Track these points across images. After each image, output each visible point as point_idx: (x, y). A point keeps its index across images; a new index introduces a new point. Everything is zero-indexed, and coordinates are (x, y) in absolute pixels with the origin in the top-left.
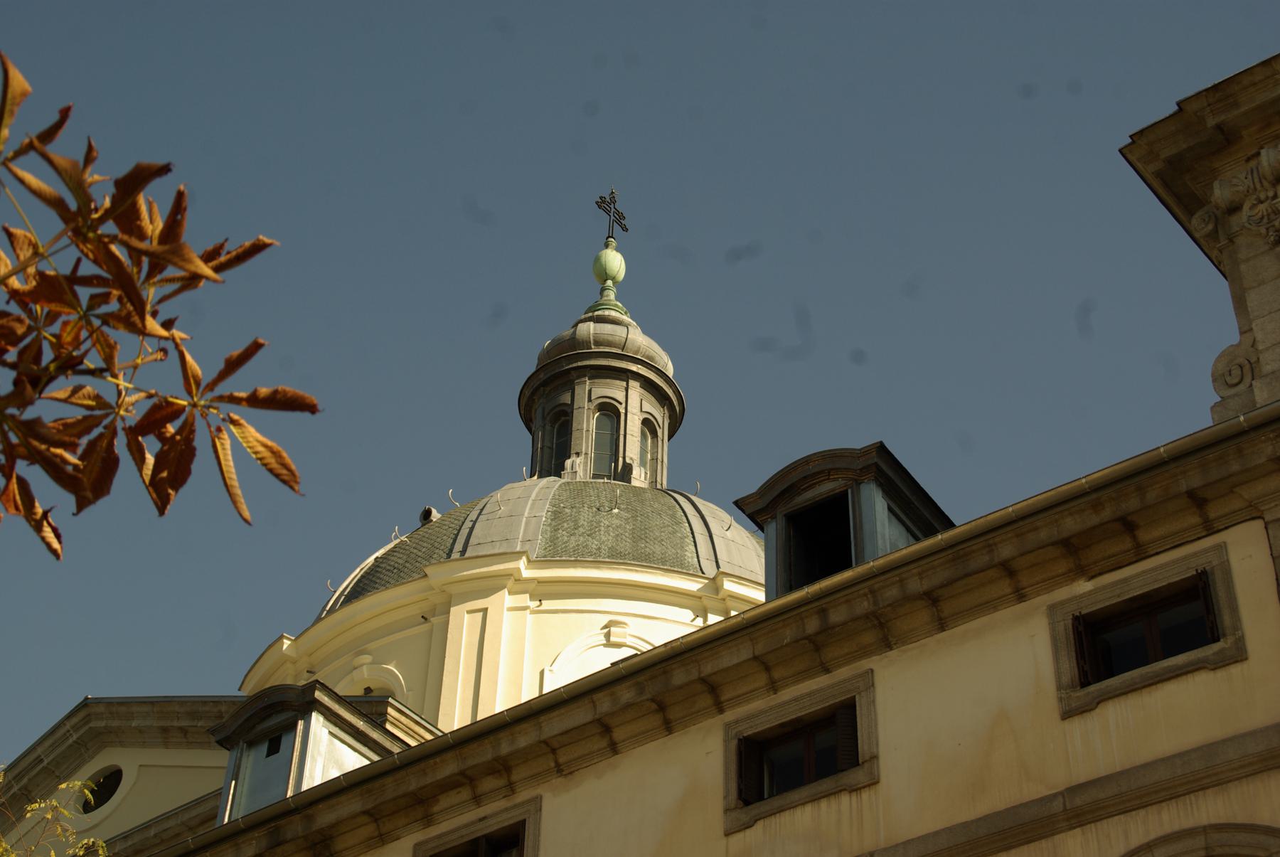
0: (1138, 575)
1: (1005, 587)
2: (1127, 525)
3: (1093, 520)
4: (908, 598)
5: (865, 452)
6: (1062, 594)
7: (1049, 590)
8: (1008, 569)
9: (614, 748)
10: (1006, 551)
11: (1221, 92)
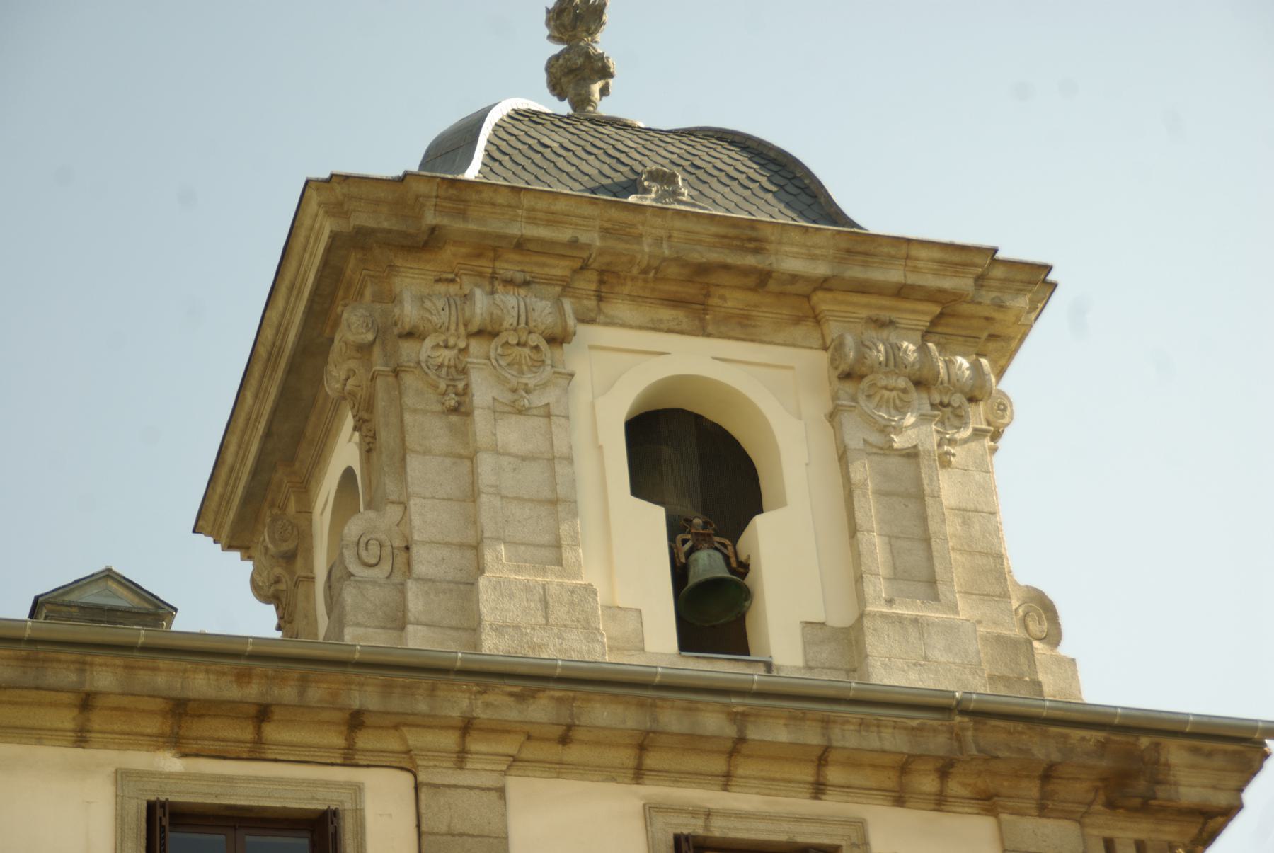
0: (249, 779)
1: (66, 719)
2: (263, 714)
3: (232, 692)
6: (140, 759)
7: (122, 747)
8: (86, 702)
10: (104, 678)
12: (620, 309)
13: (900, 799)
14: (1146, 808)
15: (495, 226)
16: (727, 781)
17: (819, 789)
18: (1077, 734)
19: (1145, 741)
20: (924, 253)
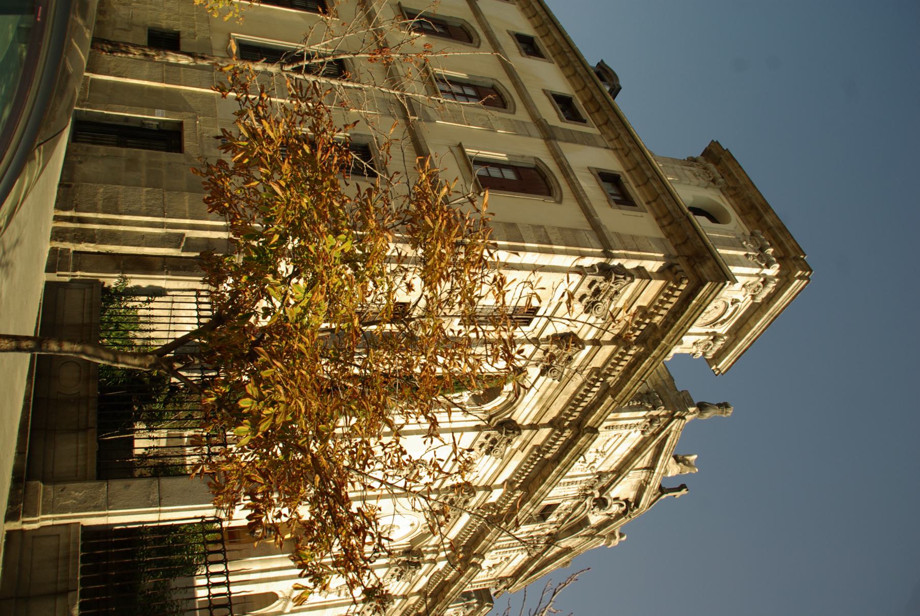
1: (579, 88)
4: (574, 67)
5: (619, 85)
9: (529, 18)
11: (731, 158)
12: (732, 201)
13: (657, 219)
14: (692, 267)
15: (730, 167)
16: (638, 186)
17: (648, 203)
18: (699, 240)
19: (708, 255)
20: (792, 242)
